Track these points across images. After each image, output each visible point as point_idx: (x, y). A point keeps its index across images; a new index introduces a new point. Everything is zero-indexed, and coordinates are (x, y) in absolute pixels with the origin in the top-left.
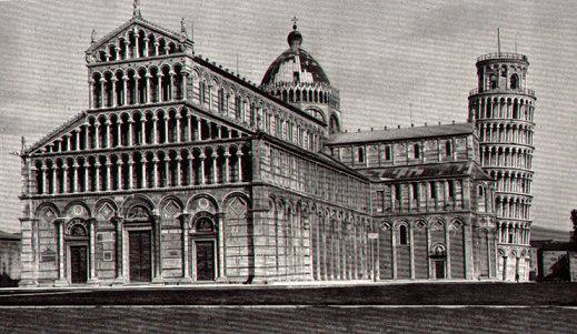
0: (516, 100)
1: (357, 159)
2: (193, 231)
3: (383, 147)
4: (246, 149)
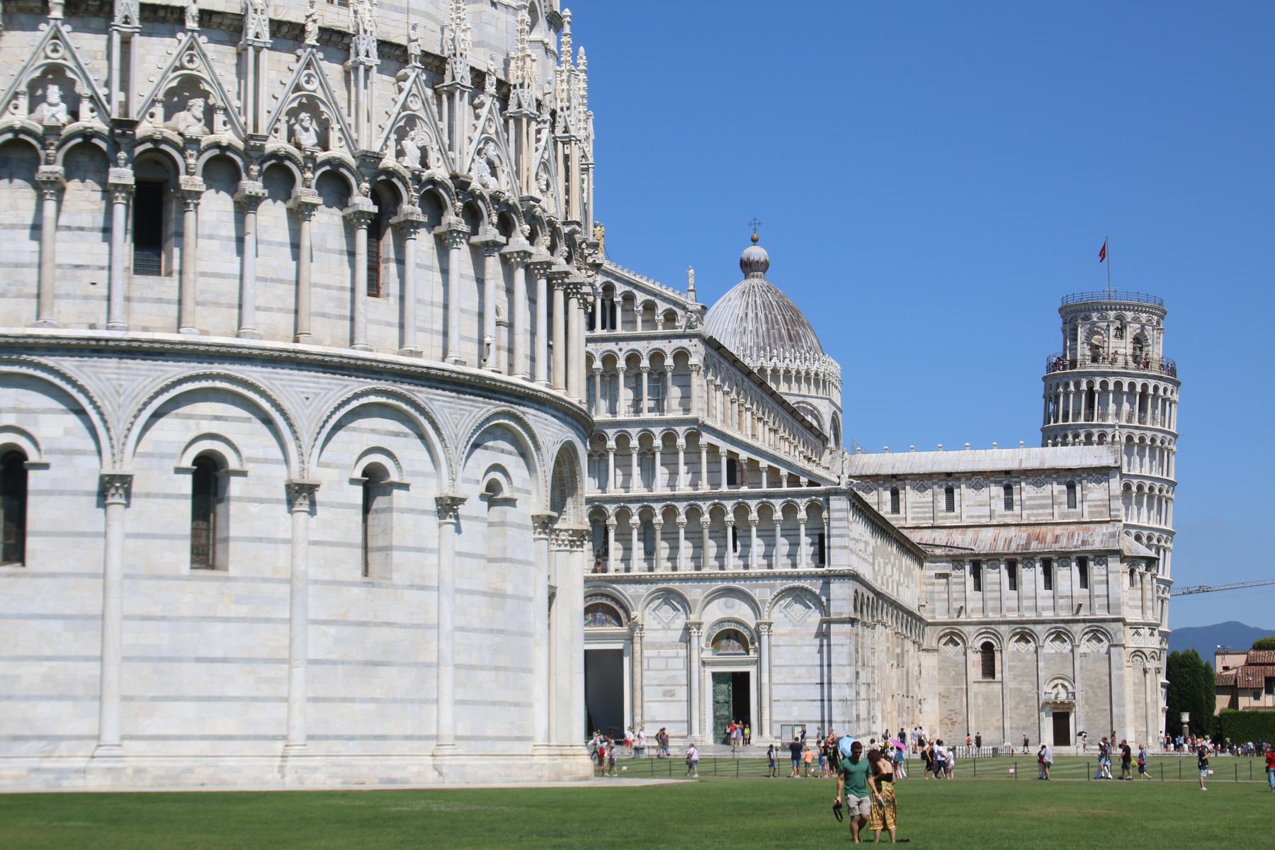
0: (1145, 386)
4: (815, 509)
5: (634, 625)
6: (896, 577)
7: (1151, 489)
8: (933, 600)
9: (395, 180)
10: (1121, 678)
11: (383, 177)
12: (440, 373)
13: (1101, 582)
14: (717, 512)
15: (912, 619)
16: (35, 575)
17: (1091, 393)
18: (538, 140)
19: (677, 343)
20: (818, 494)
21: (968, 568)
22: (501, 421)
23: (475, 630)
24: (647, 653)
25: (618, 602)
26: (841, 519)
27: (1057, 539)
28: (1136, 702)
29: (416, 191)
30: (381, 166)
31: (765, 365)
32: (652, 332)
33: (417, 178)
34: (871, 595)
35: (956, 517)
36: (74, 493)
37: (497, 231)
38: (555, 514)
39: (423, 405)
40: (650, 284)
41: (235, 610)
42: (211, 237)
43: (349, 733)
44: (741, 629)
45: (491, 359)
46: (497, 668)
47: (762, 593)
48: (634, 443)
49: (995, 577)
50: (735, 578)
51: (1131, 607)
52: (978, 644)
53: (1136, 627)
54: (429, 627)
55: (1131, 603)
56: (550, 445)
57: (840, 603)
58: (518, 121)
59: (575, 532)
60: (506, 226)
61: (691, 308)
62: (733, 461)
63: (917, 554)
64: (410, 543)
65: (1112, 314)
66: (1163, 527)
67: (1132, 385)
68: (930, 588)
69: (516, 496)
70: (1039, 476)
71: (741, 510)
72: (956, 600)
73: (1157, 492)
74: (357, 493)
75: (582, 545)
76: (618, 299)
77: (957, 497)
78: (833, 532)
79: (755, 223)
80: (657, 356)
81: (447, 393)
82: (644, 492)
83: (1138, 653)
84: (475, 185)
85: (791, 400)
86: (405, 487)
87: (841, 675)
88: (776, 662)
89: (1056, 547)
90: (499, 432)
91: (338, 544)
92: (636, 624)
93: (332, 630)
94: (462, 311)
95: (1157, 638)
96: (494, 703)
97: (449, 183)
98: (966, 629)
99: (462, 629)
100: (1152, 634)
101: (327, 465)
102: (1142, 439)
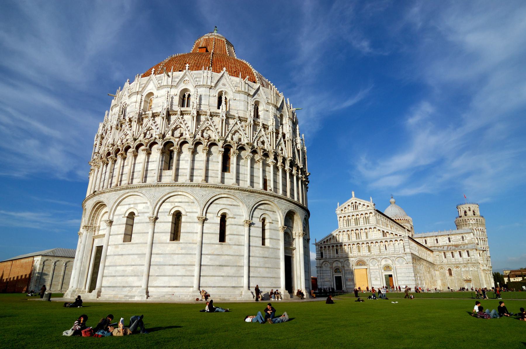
3: (435, 238)
10: (481, 275)
16: (133, 244)
23: (257, 257)
28: (486, 280)
36: (143, 223)
41: (180, 252)
42: (183, 160)
43: (213, 285)
74: (218, 220)
83: (484, 270)
91: (212, 233)
93: (209, 257)
101: (210, 213)
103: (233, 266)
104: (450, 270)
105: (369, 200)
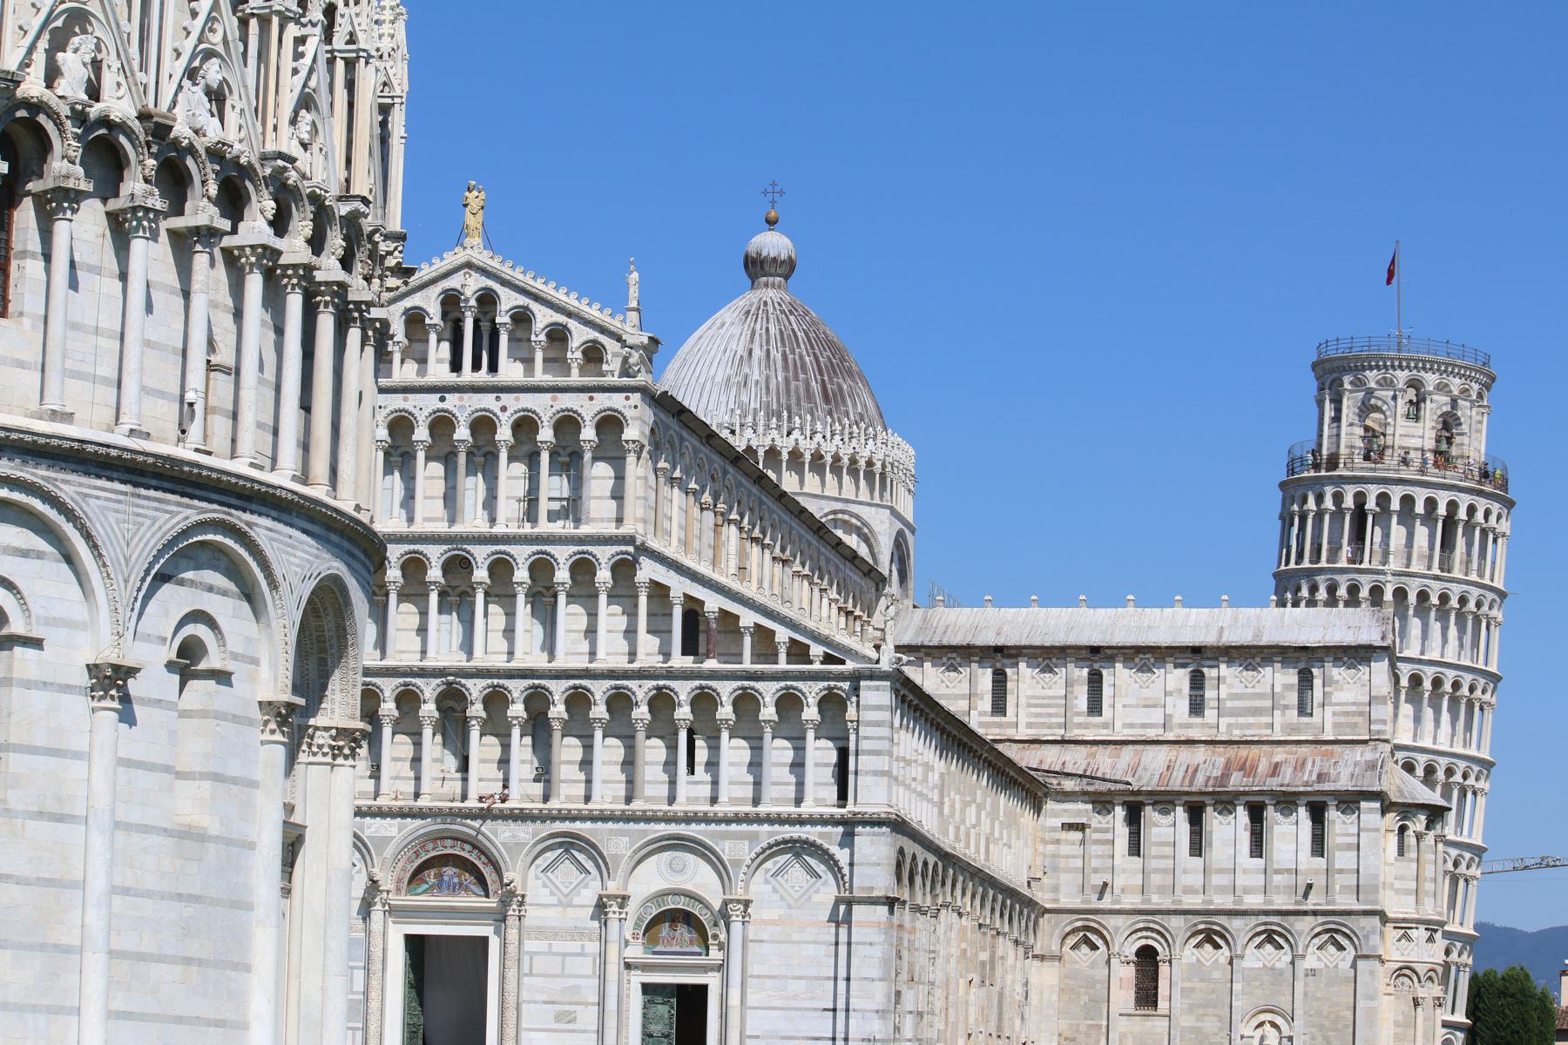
0: (1453, 506)
1: (986, 704)
2: (636, 952)
4: (832, 705)
5: (509, 896)
6: (985, 827)
7: (1456, 685)
8: (1055, 869)
9: (42, 119)
10: (1372, 1014)
11: (22, 113)
12: (102, 450)
13: (1348, 847)
14: (662, 702)
15: (1013, 904)
17: (1360, 514)
18: (298, 56)
19: (604, 401)
20: (841, 677)
21: (1120, 812)
22: (210, 537)
23: (149, 894)
24: (529, 945)
25: (483, 852)
26: (878, 724)
27: (1275, 769)
29: (78, 137)
30: (20, 93)
31: (778, 443)
32: (561, 381)
33: (80, 117)
34: (932, 859)
35: (1105, 726)
37: (214, 210)
38: (301, 701)
39: (71, 504)
40: (560, 296)
44: (696, 910)
45: (195, 430)
46: (188, 961)
47: (736, 847)
48: (521, 574)
49: (1167, 828)
50: (688, 819)
51: (1397, 891)
52: (1131, 949)
53: (1404, 926)
54: (72, 885)
55: (1398, 884)
56: (296, 581)
57: (870, 870)
58: (264, 22)
59: (342, 732)
60: (233, 201)
61: (630, 340)
62: (693, 613)
63: (1029, 788)
64: (40, 740)
65: (1402, 376)
66: (1472, 752)
67: (1431, 503)
68: (1051, 848)
69: (229, 666)
70: (1251, 656)
71: (704, 702)
72: (1096, 871)
73: (1465, 691)
75: (353, 755)
76: (503, 319)
77: (1107, 691)
78: (864, 745)
79: (774, 192)
80: (567, 424)
81: (117, 486)
82: (539, 661)
83: (1405, 971)
84: (181, 130)
85: (817, 509)
86: (36, 643)
87: (869, 995)
88: (754, 969)
89: (1273, 784)
90: (204, 556)
92: (512, 894)
94: (148, 343)
95: (1441, 943)
96: (179, 1020)
97: (136, 126)
98: (1111, 922)
99: (126, 891)
100: (1431, 940)
102: (1444, 598)
103: (30, 947)
104: (1147, 959)
105: (620, 308)
